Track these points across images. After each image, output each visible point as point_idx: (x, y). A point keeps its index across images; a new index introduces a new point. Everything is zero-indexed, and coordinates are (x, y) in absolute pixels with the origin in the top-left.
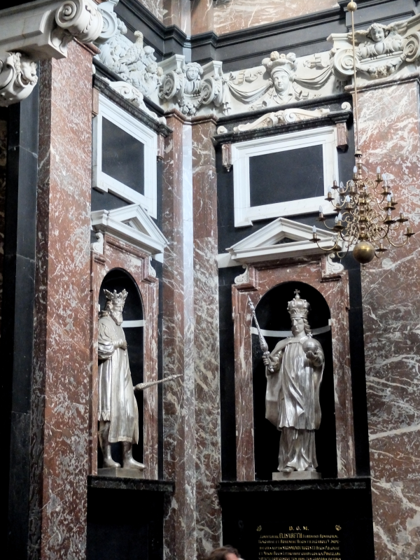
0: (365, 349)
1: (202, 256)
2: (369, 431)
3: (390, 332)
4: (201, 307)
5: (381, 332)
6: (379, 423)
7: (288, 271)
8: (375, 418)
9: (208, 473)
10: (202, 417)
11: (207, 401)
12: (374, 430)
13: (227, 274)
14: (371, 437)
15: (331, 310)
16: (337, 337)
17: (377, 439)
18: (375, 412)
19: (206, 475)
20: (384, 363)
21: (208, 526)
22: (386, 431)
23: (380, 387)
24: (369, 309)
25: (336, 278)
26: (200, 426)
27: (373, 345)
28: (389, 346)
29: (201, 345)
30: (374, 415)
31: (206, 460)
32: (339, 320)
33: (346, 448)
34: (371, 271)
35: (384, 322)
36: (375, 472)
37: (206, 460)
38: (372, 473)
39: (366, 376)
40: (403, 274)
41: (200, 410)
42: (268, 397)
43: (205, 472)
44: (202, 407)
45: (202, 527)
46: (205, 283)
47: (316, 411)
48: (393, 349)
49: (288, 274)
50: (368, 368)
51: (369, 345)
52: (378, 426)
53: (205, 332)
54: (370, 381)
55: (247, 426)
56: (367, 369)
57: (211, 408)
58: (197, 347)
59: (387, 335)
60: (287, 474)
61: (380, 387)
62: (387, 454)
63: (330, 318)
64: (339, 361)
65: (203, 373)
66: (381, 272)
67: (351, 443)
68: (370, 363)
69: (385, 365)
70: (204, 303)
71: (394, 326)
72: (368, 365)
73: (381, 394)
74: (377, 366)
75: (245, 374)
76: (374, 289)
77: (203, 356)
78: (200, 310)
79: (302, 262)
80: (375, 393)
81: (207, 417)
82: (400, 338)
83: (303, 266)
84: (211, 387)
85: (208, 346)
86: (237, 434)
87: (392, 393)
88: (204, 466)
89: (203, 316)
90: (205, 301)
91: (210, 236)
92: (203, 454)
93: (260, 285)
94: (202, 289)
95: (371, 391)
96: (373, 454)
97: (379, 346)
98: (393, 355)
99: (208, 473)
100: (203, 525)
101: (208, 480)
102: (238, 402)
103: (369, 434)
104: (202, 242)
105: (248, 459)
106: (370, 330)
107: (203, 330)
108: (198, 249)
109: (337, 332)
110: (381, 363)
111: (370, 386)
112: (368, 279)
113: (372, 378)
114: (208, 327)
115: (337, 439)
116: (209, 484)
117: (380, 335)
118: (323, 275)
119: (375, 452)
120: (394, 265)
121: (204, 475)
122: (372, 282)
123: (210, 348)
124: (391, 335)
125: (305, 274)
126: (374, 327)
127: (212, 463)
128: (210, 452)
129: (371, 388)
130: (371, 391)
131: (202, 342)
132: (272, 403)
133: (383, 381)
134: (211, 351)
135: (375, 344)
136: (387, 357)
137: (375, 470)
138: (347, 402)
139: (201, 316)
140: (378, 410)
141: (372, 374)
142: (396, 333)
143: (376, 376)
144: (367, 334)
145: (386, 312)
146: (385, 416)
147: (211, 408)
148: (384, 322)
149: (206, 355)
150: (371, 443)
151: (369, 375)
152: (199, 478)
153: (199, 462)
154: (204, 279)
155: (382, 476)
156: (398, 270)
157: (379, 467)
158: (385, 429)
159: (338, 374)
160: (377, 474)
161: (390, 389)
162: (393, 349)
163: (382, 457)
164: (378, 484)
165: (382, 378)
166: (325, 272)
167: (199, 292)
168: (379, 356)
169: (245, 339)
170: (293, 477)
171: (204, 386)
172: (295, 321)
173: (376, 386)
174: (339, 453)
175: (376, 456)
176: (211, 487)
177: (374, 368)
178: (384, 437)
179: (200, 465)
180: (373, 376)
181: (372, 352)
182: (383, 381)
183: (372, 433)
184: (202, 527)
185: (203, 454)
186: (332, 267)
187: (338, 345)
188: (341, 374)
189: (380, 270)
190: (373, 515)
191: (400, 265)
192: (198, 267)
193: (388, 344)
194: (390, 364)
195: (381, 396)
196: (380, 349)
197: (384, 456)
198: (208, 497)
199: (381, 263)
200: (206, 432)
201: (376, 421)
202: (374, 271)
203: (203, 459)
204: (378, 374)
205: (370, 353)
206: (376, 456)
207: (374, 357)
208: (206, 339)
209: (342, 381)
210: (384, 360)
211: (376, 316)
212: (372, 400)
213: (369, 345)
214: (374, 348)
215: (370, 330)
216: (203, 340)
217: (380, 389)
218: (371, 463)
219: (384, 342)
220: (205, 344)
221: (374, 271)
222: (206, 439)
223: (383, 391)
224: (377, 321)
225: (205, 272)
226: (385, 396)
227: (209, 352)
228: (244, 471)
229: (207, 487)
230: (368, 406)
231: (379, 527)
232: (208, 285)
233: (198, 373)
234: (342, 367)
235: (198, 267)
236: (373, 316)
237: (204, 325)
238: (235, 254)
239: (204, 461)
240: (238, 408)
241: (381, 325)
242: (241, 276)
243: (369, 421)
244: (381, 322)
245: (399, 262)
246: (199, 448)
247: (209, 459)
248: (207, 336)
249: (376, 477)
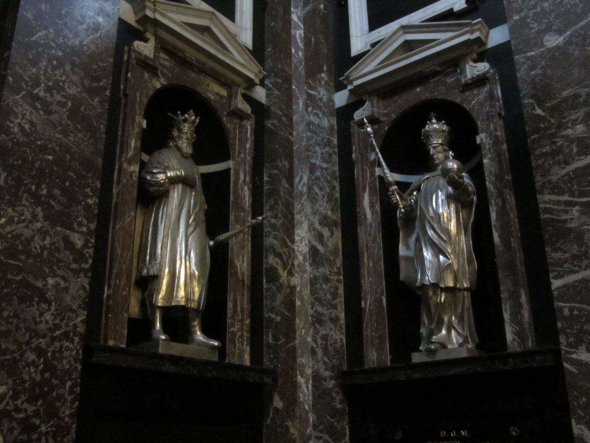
0: (532, 158)
1: (315, 96)
2: (551, 275)
3: (567, 127)
4: (315, 153)
5: (554, 130)
6: (566, 261)
7: (418, 90)
8: (558, 255)
9: (326, 359)
10: (318, 286)
11: (323, 265)
12: (559, 272)
13: (345, 114)
14: (556, 284)
15: (479, 123)
16: (489, 156)
17: (565, 286)
18: (558, 245)
19: (325, 363)
20: (564, 172)
21: (327, 433)
22: (577, 272)
23: (562, 207)
24: (532, 104)
25: (481, 81)
26: (316, 299)
27: (544, 150)
28: (568, 146)
29: (315, 198)
30: (556, 250)
31: (324, 343)
32: (491, 134)
33: (517, 308)
34: (529, 54)
35: (556, 116)
36: (567, 338)
37: (324, 343)
38: (562, 339)
39: (538, 196)
40: (577, 45)
41: (315, 278)
42: (402, 251)
43: (322, 358)
44: (317, 274)
45: (320, 434)
46: (319, 125)
47: (470, 263)
48: (575, 150)
49: (420, 93)
50: (540, 183)
51: (538, 152)
52: (565, 266)
53: (320, 181)
54: (545, 202)
55: (377, 293)
56: (538, 185)
57: (328, 273)
58: (311, 201)
59: (564, 133)
60: (430, 352)
61: (562, 207)
62: (585, 306)
63: (477, 134)
64: (496, 187)
65: (318, 231)
66: (543, 52)
67: (524, 298)
68: (542, 176)
69: (566, 175)
70: (317, 148)
71: (572, 117)
72: (539, 180)
73: (564, 217)
74: (554, 178)
75: (371, 226)
76: (536, 76)
77: (317, 210)
78: (313, 157)
79: (434, 74)
80: (555, 217)
81: (324, 286)
82: (584, 132)
83: (436, 79)
84: (328, 247)
85: (323, 196)
86: (363, 305)
87: (582, 213)
88: (321, 350)
89: (318, 163)
90: (319, 145)
91: (322, 71)
92: (320, 335)
93: (385, 115)
94: (315, 132)
95: (548, 216)
96: (561, 309)
97: (553, 150)
98: (577, 158)
99: (326, 359)
100: (321, 431)
101: (326, 370)
102: (364, 263)
103: (552, 280)
104: (314, 81)
105: (379, 337)
106: (537, 130)
107: (318, 178)
108: (310, 90)
109: (490, 149)
110: (558, 173)
111: (546, 208)
112: (526, 67)
113: (547, 197)
114: (322, 174)
115: (502, 296)
116: (327, 374)
117: (554, 135)
118: (463, 80)
119: (564, 307)
120: (561, 39)
121: (321, 362)
122: (532, 68)
123: (326, 199)
124: (569, 132)
125: (440, 88)
126: (542, 125)
127: (331, 345)
128: (328, 331)
129: (547, 210)
130: (548, 216)
131: (317, 194)
132: (408, 259)
133: (566, 198)
134: (327, 203)
135: (547, 149)
136: (567, 163)
137: (566, 334)
138: (512, 240)
139: (314, 164)
140: (562, 241)
141: (546, 191)
142: (578, 126)
143: (554, 193)
144: (533, 137)
145: (560, 102)
146: (575, 249)
147: (328, 273)
148: (556, 116)
149: (321, 209)
150: (556, 293)
151: (541, 193)
152: (316, 367)
153: (315, 346)
154: (316, 121)
155: (576, 346)
156: (568, 43)
157: (572, 330)
158: (577, 269)
159: (496, 204)
160: (571, 340)
161: (577, 208)
162: (575, 150)
163: (576, 312)
164: (574, 356)
165: (563, 194)
166: (465, 77)
167: (313, 137)
168: (554, 164)
169: (369, 183)
170: (441, 356)
171: (320, 247)
172: (431, 149)
173: (555, 207)
174: (506, 316)
175: (566, 312)
176: (331, 378)
177: (549, 182)
178: (576, 281)
179: (317, 350)
180: (549, 194)
181: (543, 160)
182: (566, 198)
183: (555, 278)
184: (320, 434)
185: (320, 335)
186: (475, 69)
187: (491, 165)
188: (500, 204)
189: (542, 49)
190: (571, 407)
191: (571, 36)
192: (310, 109)
193: (566, 144)
194: (574, 171)
195: (565, 221)
196: (555, 153)
197: (580, 310)
198: (327, 392)
199: (542, 42)
200: (323, 306)
201: (561, 259)
202: (533, 53)
203: (319, 341)
204: (556, 189)
205: (540, 162)
206: (566, 312)
207: (548, 167)
208: (321, 189)
209: (503, 213)
210: (564, 168)
211: (544, 111)
212: (550, 228)
213: (538, 152)
214: (544, 155)
215: (537, 130)
216: (317, 191)
217: (563, 211)
218: (559, 325)
219: (559, 144)
220: (320, 195)
221: (533, 53)
222: (323, 314)
223: (566, 212)
224: (545, 117)
225: (318, 112)
226: (572, 219)
227: (325, 204)
228: (375, 354)
229: (325, 379)
230: (545, 237)
231: (583, 427)
232: (322, 126)
233: (313, 232)
234: (500, 195)
235: (310, 109)
236: (539, 112)
237: (318, 174)
238: (351, 82)
239: (322, 344)
240: (364, 271)
241: (553, 121)
242: (361, 109)
243: (549, 261)
244: (553, 117)
245: (568, 33)
246: (315, 328)
247: (327, 340)
248: (322, 185)
249: (569, 345)
